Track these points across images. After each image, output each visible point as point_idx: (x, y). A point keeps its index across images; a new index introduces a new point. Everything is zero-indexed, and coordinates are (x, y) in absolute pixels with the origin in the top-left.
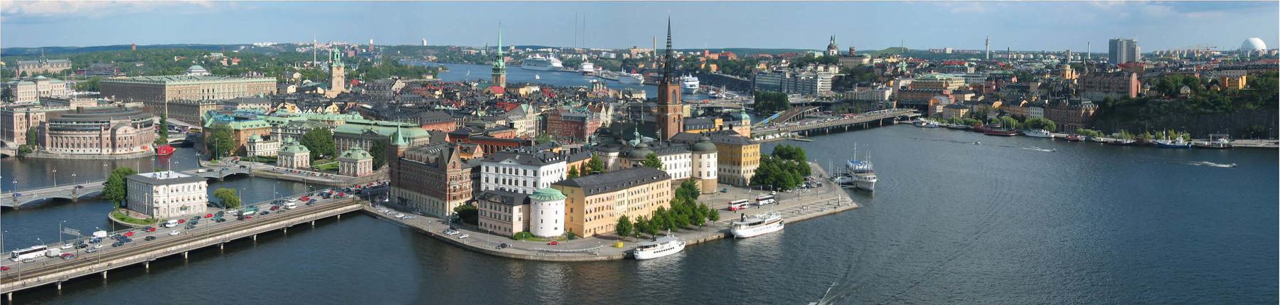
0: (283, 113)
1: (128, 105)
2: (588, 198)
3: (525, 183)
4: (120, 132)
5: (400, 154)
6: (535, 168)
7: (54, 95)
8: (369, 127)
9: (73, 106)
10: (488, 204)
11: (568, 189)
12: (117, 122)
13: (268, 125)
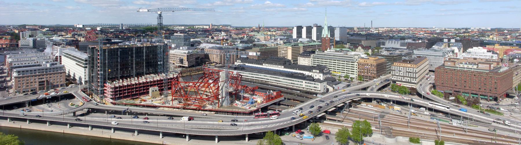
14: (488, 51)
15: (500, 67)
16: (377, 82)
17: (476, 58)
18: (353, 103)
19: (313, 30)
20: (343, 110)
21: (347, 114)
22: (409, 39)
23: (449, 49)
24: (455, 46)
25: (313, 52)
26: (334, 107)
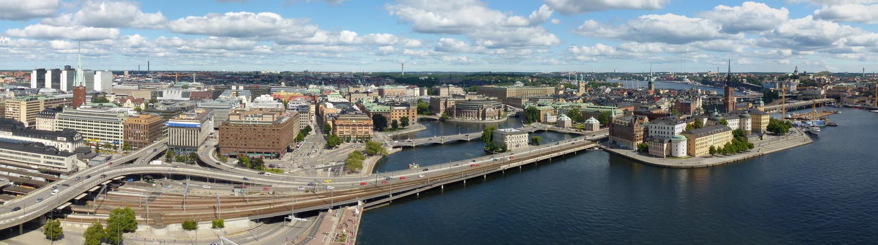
0: (559, 103)
1: (491, 98)
2: (697, 139)
3: (668, 133)
4: (487, 110)
5: (613, 122)
6: (673, 126)
7: (458, 93)
8: (597, 109)
9: (467, 99)
10: (653, 143)
11: (688, 135)
12: (486, 106)
13: (552, 108)
14: (274, 100)
15: (283, 118)
16: (149, 150)
17: (262, 108)
18: (114, 185)
19: (61, 75)
20: (97, 196)
21: (103, 201)
22: (193, 87)
23: (237, 98)
24: (243, 95)
25: (60, 109)
26: (85, 193)
